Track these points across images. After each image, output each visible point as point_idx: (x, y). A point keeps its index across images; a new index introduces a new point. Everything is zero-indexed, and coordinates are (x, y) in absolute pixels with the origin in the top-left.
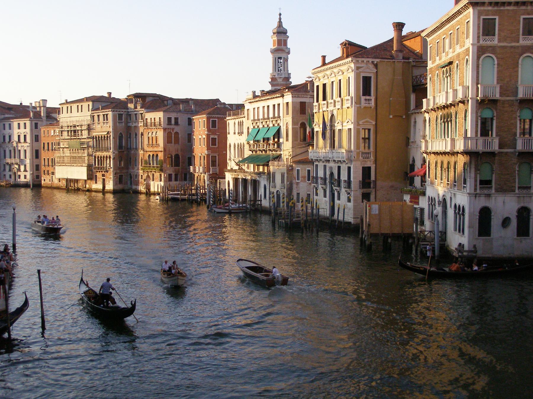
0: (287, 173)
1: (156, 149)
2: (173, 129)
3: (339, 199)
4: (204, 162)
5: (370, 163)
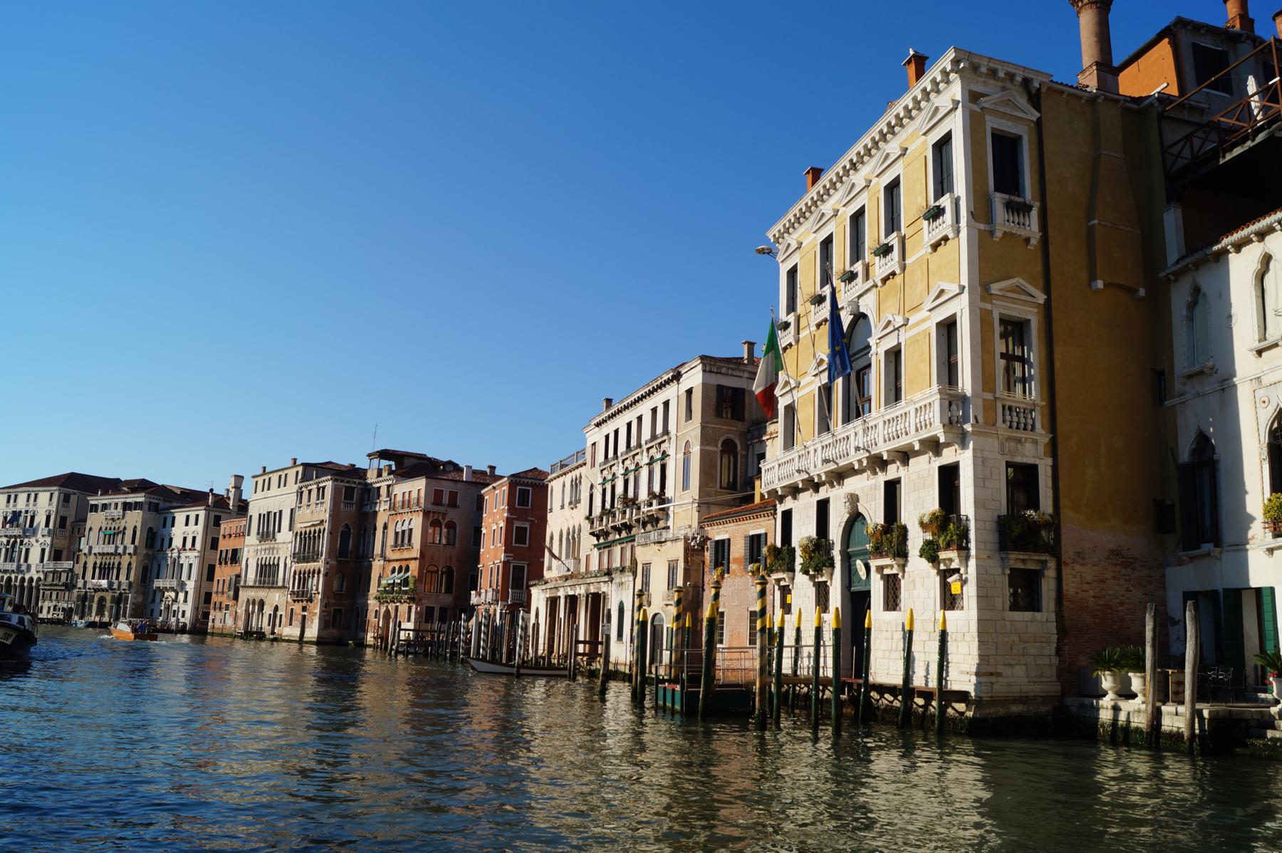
0: (686, 561)
1: (406, 555)
2: (444, 515)
3: (892, 601)
4: (497, 579)
5: (1033, 451)
